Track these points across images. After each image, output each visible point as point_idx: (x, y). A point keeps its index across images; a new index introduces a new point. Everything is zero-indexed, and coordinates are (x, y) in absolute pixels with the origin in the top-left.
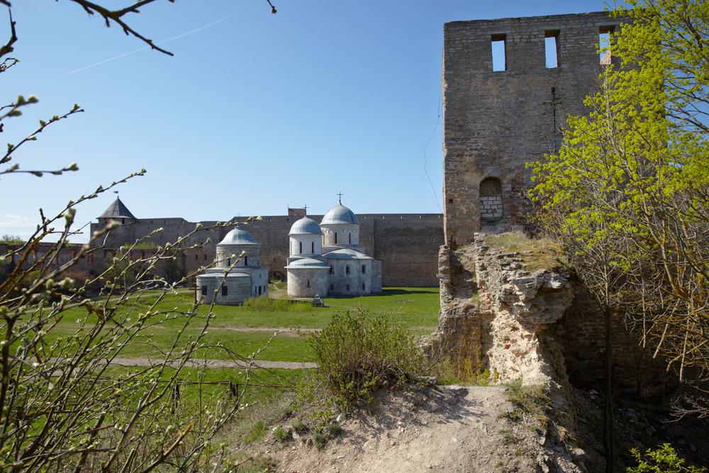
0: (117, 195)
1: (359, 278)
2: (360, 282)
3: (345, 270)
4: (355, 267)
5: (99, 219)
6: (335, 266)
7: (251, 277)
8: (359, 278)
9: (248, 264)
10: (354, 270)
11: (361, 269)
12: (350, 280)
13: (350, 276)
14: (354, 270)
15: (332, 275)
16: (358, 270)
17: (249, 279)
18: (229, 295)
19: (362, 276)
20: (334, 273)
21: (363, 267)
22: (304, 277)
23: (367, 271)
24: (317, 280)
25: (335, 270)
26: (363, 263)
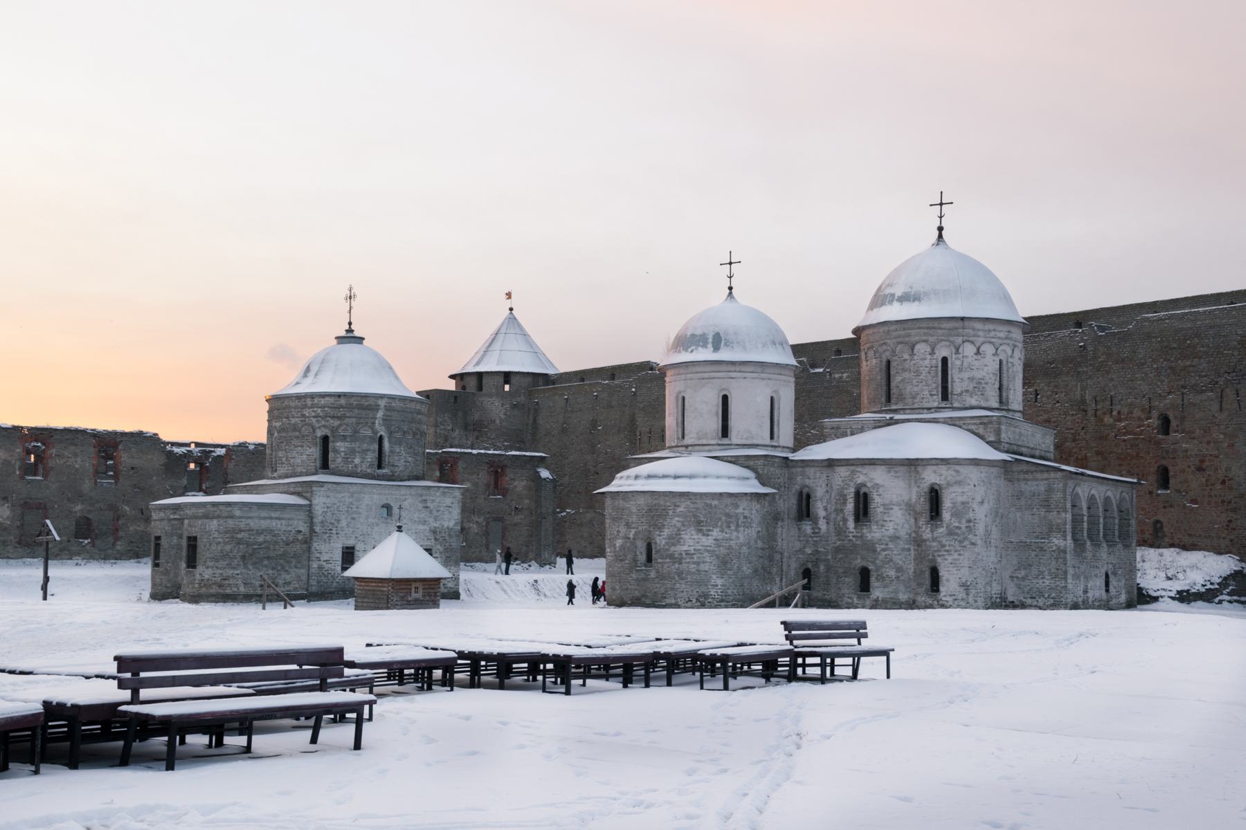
0: (508, 304)
1: (918, 542)
2: (919, 558)
3: (850, 506)
4: (893, 494)
5: (459, 377)
6: (820, 492)
7: (310, 505)
8: (918, 542)
9: (331, 466)
10: (887, 507)
11: (923, 505)
12: (871, 548)
13: (874, 533)
14: (887, 507)
15: (807, 527)
16: (909, 507)
17: (303, 515)
18: (200, 569)
19: (927, 534)
20: (815, 521)
21: (935, 498)
22: (628, 525)
23: (946, 515)
24: (675, 539)
25: (819, 509)
26: (930, 477)
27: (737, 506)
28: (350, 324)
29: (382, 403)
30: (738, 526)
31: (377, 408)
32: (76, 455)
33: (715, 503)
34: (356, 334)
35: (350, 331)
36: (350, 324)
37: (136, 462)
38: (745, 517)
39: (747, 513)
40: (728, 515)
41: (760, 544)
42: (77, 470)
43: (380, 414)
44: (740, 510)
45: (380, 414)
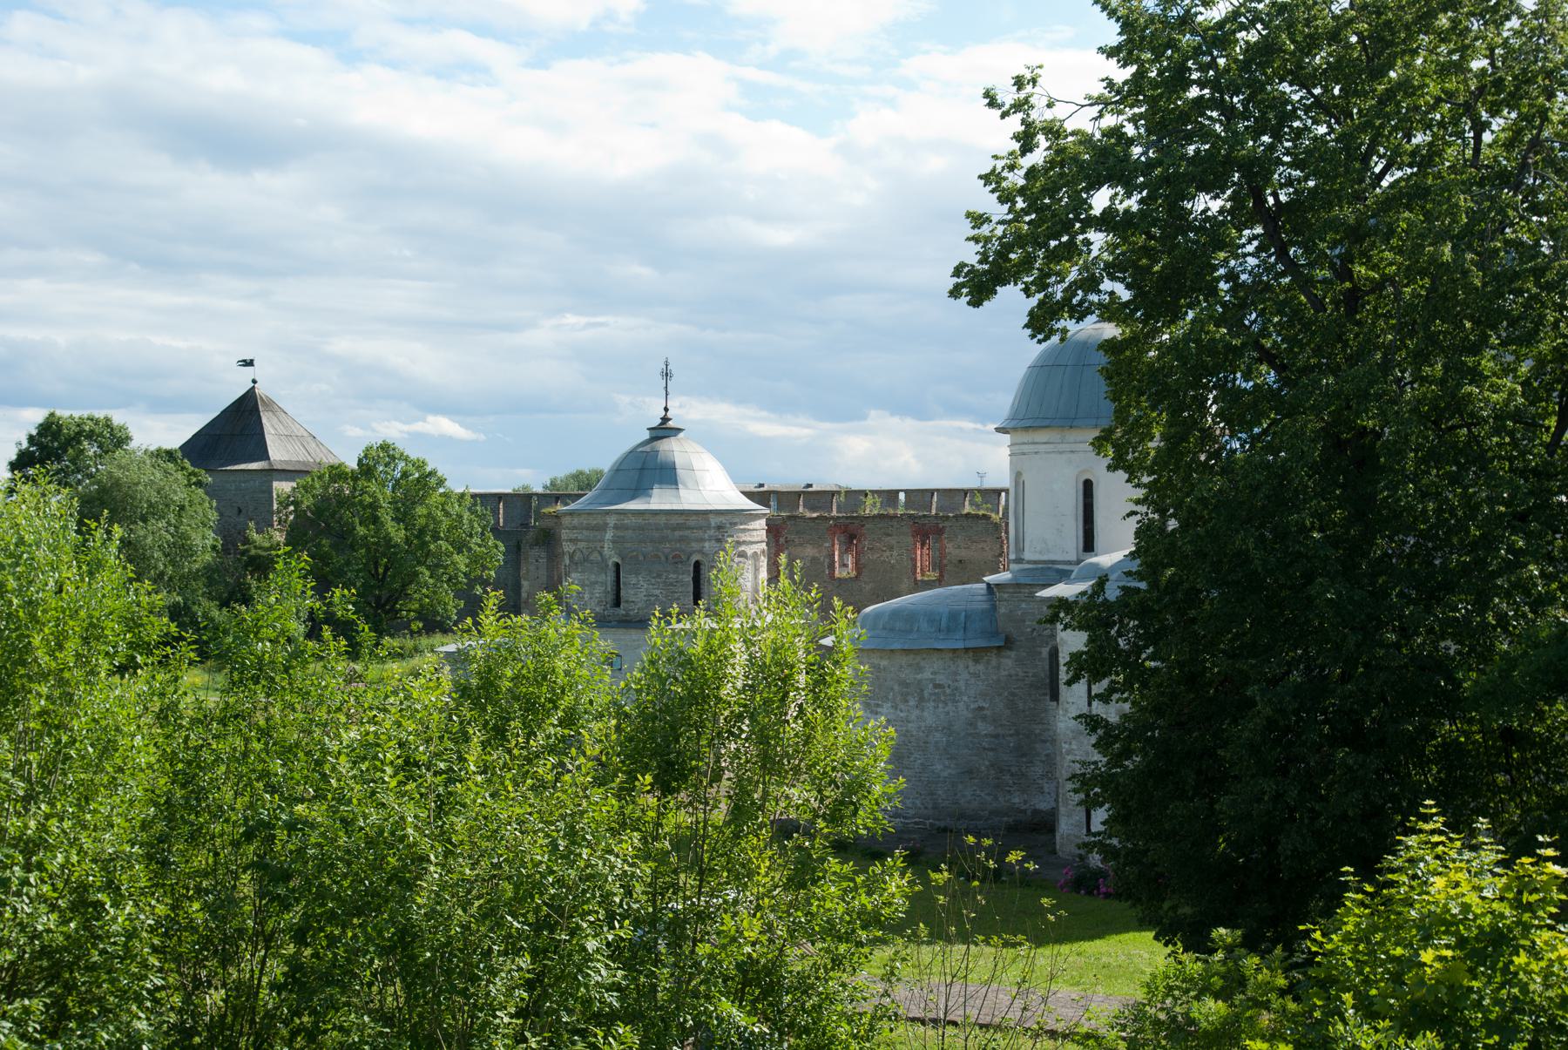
27: (920, 669)
28: (666, 409)
29: (612, 521)
30: (922, 699)
31: (602, 528)
32: (891, 548)
33: (884, 663)
34: (671, 424)
35: (665, 420)
36: (666, 409)
37: (964, 554)
38: (936, 686)
39: (941, 679)
40: (904, 684)
41: (983, 728)
42: (893, 567)
43: (609, 535)
44: (927, 675)
45: (609, 535)
